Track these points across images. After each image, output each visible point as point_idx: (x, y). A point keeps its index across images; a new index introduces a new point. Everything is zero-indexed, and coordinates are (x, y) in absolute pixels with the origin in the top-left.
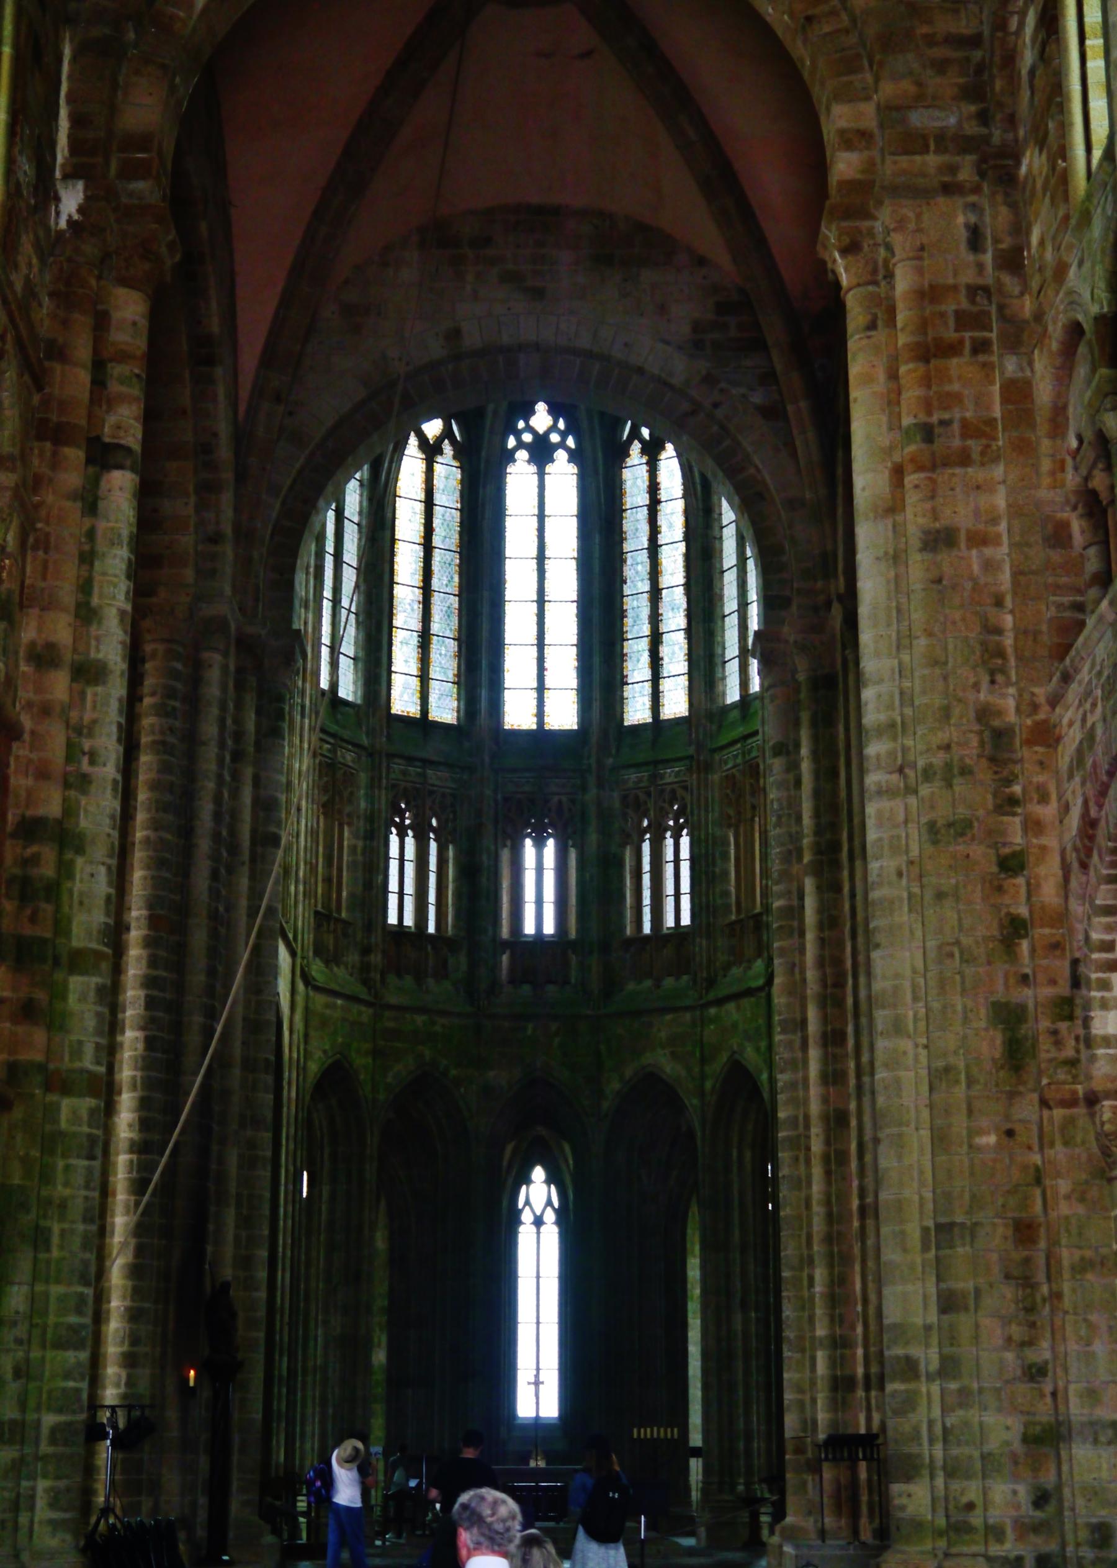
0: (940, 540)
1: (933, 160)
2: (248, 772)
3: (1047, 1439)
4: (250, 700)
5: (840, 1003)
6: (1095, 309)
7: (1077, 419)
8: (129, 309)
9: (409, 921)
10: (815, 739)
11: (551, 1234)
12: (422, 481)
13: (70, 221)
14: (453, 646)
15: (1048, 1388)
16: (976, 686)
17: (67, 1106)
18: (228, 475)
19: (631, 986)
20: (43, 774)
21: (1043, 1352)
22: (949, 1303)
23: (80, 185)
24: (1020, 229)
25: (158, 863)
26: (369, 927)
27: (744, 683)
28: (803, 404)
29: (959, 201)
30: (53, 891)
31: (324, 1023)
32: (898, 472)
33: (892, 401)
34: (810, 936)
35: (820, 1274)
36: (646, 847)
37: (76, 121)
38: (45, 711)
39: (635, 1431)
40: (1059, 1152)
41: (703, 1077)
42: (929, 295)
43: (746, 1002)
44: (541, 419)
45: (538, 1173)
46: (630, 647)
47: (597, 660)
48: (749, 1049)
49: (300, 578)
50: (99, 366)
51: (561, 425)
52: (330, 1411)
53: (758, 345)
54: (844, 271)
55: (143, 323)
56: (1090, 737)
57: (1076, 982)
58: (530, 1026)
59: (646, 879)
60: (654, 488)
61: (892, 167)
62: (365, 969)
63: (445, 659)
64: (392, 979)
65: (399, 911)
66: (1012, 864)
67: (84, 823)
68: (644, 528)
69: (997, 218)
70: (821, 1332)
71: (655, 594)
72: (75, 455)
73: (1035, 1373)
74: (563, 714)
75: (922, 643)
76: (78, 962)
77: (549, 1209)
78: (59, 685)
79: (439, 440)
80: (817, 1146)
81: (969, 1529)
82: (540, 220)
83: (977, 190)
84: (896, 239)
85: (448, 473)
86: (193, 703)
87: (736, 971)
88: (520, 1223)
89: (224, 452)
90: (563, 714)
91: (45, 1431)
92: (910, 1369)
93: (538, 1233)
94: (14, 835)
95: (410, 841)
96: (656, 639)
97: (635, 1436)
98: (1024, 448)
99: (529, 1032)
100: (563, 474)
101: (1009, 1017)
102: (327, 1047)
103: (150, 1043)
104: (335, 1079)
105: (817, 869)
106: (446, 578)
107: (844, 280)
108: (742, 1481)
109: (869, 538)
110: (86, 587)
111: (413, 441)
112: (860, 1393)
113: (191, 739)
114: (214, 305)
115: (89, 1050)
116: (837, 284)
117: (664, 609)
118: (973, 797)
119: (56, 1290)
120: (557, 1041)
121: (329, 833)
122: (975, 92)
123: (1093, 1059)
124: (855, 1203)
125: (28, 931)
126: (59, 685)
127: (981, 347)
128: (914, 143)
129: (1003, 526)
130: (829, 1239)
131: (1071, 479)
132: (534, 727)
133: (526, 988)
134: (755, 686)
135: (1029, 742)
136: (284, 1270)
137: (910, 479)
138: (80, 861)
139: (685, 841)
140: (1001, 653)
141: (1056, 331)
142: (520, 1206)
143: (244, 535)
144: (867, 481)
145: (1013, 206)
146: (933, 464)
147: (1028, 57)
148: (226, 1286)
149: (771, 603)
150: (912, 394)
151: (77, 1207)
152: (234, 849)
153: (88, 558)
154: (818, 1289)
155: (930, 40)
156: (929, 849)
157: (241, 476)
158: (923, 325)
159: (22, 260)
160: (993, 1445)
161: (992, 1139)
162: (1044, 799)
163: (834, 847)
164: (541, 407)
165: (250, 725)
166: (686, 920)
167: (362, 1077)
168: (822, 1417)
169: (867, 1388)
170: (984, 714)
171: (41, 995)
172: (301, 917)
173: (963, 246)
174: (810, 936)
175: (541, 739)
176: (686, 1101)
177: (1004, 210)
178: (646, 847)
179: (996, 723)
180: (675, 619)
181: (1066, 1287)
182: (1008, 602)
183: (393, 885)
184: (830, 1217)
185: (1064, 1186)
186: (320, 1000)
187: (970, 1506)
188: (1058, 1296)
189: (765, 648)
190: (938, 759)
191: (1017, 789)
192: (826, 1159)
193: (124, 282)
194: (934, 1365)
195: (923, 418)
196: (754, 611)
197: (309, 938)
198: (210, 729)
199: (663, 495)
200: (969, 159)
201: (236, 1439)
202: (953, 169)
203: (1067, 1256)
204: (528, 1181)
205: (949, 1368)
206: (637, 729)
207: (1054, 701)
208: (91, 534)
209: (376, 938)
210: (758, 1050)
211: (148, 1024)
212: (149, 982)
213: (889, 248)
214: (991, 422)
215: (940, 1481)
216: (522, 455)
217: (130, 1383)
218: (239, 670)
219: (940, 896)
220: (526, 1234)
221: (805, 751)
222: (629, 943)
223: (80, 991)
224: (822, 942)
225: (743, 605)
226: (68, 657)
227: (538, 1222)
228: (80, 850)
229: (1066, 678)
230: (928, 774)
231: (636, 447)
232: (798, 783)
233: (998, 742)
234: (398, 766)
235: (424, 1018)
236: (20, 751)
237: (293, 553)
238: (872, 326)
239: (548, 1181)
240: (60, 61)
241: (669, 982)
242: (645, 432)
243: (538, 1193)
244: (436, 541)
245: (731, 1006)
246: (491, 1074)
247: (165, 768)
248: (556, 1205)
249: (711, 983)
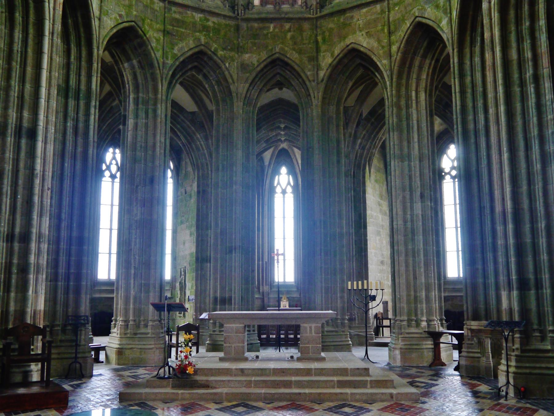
11: (290, 198)
39: (349, 283)
41: (390, 45)
45: (284, 170)
48: (429, 9)
52: (133, 272)
58: (272, 26)
77: (289, 186)
88: (275, 192)
93: (284, 197)
97: (350, 288)
99: (271, 30)
102: (123, 13)
108: (424, 318)
120: (289, 35)
133: (270, 7)
136: (45, 142)
142: (275, 185)
167: (154, 45)
176: (378, 63)
204: (279, 173)
210: (437, 7)
220: (278, 198)
227: (284, 192)
235: (199, 15)
239: (288, 174)
243: (284, 179)
246: (247, 56)
248: (292, 184)
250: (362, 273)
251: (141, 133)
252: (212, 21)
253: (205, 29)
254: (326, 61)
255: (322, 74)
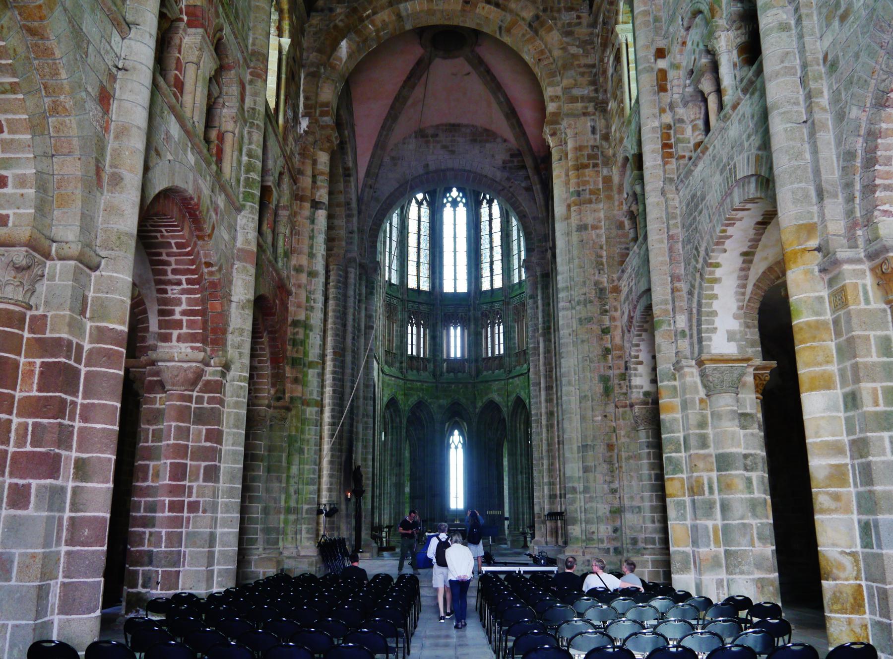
0: (582, 228)
1: (580, 105)
2: (364, 306)
3: (617, 512)
4: (364, 283)
5: (551, 377)
6: (632, 152)
7: (627, 188)
8: (323, 158)
9: (415, 353)
10: (543, 293)
11: (461, 451)
12: (417, 214)
13: (305, 131)
14: (427, 266)
15: (618, 496)
16: (594, 274)
17: (309, 410)
18: (355, 212)
19: (485, 373)
20: (299, 306)
21: (615, 485)
22: (586, 470)
23: (307, 119)
24: (608, 127)
25: (336, 335)
26: (402, 355)
27: (520, 276)
28: (538, 186)
29: (588, 118)
30: (303, 343)
31: (388, 385)
32: (569, 206)
33: (567, 183)
34: (541, 356)
35: (545, 462)
36: (489, 329)
37: (306, 98)
38: (299, 286)
40: (621, 422)
41: (508, 401)
42: (579, 148)
43: (521, 378)
44: (455, 193)
45: (456, 432)
46: (483, 266)
47: (473, 270)
49: (379, 244)
50: (314, 176)
51: (461, 195)
53: (524, 167)
54: (551, 142)
55: (328, 163)
56: (631, 290)
57: (626, 369)
59: (489, 339)
60: (490, 215)
61: (567, 107)
62: (401, 368)
63: (425, 270)
64: (409, 371)
65: (412, 350)
66: (605, 331)
67: (312, 322)
68: (488, 228)
69: (601, 124)
70: (546, 480)
71: (491, 248)
72: (307, 205)
73: (614, 491)
74: (463, 288)
75: (576, 261)
76: (311, 365)
78: (304, 278)
79: (422, 201)
80: (544, 422)
81: (593, 540)
82: (453, 128)
83: (594, 114)
84: (568, 131)
85: (425, 211)
86: (346, 284)
87: (518, 368)
89: (354, 205)
90: (463, 288)
91: (304, 511)
92: (574, 490)
94: (290, 326)
95: (414, 328)
96: (492, 263)
98: (609, 198)
100: (462, 210)
101: (605, 380)
103: (334, 391)
104: (392, 403)
105: (544, 335)
106: (425, 244)
107: (551, 145)
109: (560, 228)
110: (311, 247)
111: (414, 201)
112: (558, 499)
113: (345, 296)
114: (350, 158)
115: (315, 393)
116: (549, 147)
117: (494, 253)
118: (593, 310)
119: (307, 467)
121: (389, 325)
122: (594, 83)
123: (632, 392)
124: (556, 440)
125: (295, 355)
126: (304, 278)
127: (595, 165)
128: (574, 100)
129: (603, 223)
130: (548, 451)
131: (625, 208)
132: (453, 291)
133: (452, 374)
134: (523, 277)
135: (611, 292)
137: (572, 209)
138: (311, 333)
139: (501, 327)
140: (602, 264)
141: (620, 160)
143: (361, 231)
144: (559, 209)
145: (606, 119)
146: (580, 204)
147: (610, 71)
148: (359, 467)
149: (528, 250)
150: (573, 181)
151: (312, 442)
152: (359, 330)
153: (312, 238)
154: (545, 467)
155: (579, 66)
156: (579, 327)
157: (359, 213)
158: (577, 159)
159: (289, 143)
160: (600, 514)
161: (600, 418)
162: (616, 310)
163: (549, 328)
164: (454, 189)
165: (364, 291)
166: (502, 352)
168: (547, 507)
169: (561, 498)
170: (596, 283)
171: (300, 376)
172: (381, 352)
173: (590, 133)
174: (541, 356)
175: (455, 295)
177: (603, 121)
178: (489, 329)
179: (601, 286)
180: (498, 256)
181: (624, 464)
182: (605, 247)
183: (409, 342)
184: (548, 444)
185: (623, 433)
186: (387, 378)
187: (593, 533)
188: (621, 467)
189: (527, 265)
190: (582, 298)
191: (607, 307)
192: (547, 426)
193: (321, 150)
194: (582, 489)
195: (577, 189)
196: (523, 253)
197: (383, 359)
198: (351, 293)
199: (493, 217)
200: (592, 104)
201: (363, 514)
202: (586, 108)
203: (624, 455)
205: (586, 490)
206: (485, 292)
207: (619, 279)
208: (313, 230)
209: (404, 358)
211: (334, 385)
212: (334, 372)
213: (566, 134)
214: (599, 190)
215: (583, 525)
216: (449, 205)
217: (330, 497)
218: (360, 274)
219: (583, 341)
221: (539, 297)
222: (484, 359)
223: (312, 374)
224: (545, 358)
225: (519, 251)
226: (306, 269)
227: (456, 448)
228: (311, 330)
229: (623, 271)
230: (579, 303)
231: (485, 201)
232: (537, 307)
233: (601, 292)
234: (410, 304)
236: (292, 299)
237: (377, 237)
238: (560, 159)
240: (300, 79)
241: (497, 371)
242: (488, 196)
243: (456, 439)
244: (422, 233)
245: (516, 379)
247: (337, 305)
249: (510, 372)
250: (501, 507)
251: (394, 442)
252: (425, 386)
253: (422, 389)
254: (479, 404)
255: (477, 410)
